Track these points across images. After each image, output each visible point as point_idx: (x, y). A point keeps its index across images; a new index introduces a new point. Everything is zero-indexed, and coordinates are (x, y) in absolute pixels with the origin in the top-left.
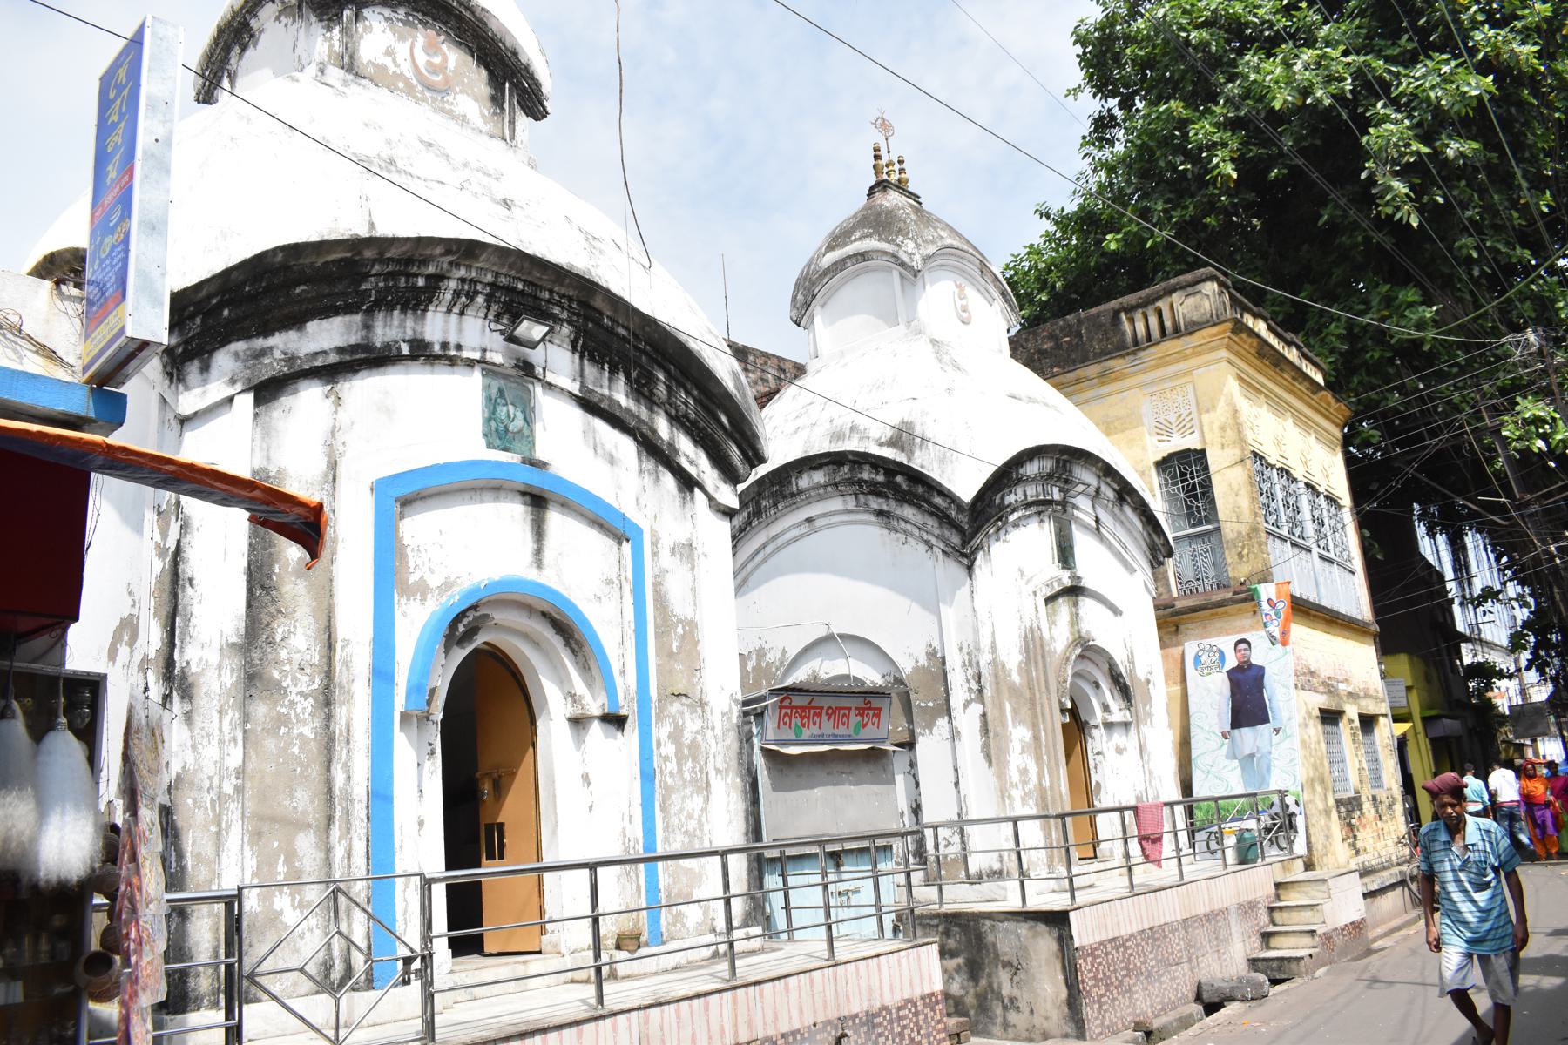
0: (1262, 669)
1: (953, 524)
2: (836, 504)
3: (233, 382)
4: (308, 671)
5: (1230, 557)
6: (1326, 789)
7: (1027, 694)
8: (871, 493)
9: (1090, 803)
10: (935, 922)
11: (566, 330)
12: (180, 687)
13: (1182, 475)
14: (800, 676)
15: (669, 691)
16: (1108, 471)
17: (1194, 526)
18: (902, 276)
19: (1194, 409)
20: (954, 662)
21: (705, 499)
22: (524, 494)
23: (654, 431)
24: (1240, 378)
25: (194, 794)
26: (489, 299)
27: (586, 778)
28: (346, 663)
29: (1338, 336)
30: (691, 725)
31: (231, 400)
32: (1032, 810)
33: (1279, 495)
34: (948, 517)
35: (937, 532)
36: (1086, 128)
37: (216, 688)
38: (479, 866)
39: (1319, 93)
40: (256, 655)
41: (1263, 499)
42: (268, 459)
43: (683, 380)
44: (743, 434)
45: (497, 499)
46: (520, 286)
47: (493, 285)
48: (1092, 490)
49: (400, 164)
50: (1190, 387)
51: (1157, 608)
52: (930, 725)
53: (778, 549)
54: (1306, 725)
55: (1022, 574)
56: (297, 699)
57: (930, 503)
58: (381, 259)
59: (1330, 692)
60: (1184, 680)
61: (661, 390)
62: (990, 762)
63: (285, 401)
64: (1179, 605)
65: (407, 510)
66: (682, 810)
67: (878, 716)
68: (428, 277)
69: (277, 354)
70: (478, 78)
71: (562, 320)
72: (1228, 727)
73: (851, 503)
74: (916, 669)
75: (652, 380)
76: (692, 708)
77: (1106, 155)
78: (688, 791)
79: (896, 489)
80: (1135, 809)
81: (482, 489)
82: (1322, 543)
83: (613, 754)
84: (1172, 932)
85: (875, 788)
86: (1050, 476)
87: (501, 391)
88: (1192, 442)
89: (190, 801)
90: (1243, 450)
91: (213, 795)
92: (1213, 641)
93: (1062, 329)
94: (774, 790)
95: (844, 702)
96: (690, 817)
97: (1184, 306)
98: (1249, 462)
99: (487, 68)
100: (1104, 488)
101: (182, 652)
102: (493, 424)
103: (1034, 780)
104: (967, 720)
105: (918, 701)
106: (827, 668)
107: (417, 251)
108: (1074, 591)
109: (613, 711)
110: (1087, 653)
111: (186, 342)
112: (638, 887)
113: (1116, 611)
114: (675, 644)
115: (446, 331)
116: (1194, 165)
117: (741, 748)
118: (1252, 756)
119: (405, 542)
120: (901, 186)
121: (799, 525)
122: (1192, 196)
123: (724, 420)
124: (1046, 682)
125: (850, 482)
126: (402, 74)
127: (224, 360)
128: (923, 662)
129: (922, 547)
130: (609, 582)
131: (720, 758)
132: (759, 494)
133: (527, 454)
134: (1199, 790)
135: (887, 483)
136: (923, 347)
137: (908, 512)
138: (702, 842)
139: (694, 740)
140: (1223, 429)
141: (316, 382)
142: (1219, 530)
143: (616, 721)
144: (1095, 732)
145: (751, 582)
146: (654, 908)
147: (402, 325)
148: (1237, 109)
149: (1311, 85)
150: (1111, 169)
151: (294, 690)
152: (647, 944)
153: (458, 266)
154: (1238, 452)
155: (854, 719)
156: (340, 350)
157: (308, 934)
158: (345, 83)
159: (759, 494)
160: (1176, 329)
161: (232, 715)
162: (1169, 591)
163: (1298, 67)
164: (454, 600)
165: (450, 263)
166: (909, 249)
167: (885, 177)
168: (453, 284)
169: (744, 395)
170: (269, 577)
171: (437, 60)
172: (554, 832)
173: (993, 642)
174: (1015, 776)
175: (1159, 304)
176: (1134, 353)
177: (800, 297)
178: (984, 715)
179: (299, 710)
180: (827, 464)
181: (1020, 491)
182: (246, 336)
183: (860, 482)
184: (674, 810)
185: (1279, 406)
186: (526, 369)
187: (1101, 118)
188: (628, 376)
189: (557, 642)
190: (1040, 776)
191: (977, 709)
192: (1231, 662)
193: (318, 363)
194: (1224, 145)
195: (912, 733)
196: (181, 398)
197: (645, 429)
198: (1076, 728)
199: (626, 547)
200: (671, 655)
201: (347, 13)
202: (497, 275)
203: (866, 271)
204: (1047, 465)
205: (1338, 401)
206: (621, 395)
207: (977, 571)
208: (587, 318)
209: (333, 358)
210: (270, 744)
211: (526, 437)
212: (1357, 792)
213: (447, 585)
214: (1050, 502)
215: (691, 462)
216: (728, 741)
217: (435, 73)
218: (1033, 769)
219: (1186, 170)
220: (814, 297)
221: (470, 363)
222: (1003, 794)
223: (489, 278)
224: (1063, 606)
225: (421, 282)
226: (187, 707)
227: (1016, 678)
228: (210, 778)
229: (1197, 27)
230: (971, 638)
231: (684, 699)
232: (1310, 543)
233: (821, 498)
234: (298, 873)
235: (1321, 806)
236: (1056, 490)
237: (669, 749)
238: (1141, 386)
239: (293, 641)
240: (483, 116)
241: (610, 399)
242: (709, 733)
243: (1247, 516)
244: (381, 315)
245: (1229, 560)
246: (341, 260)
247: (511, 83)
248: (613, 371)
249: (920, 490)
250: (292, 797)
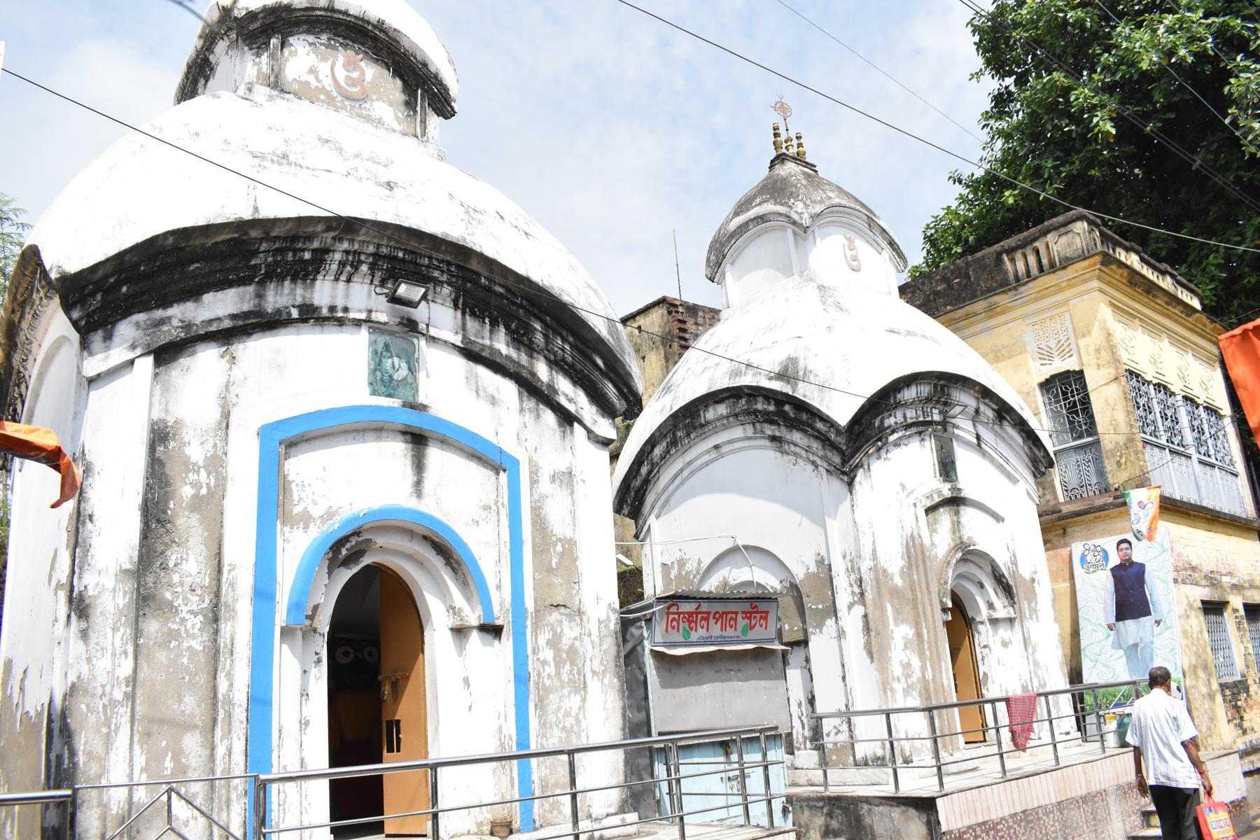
0: (1142, 566)
1: (834, 446)
2: (738, 432)
3: (133, 347)
4: (199, 592)
5: (1109, 465)
6: (1209, 675)
7: (910, 596)
8: (766, 421)
9: (979, 694)
10: (821, 804)
11: (446, 290)
12: (77, 608)
13: (1064, 393)
14: (711, 585)
15: (547, 603)
16: (985, 393)
17: (1074, 439)
18: (795, 233)
19: (1071, 335)
20: (839, 568)
21: (584, 432)
22: (404, 433)
23: (534, 375)
24: (1112, 304)
25: (88, 700)
26: (373, 267)
27: (466, 681)
28: (232, 585)
29: (1218, 266)
30: (569, 632)
31: (132, 362)
32: (915, 702)
33: (1157, 409)
34: (828, 439)
35: (821, 453)
36: (987, 105)
37: (110, 608)
38: (381, 762)
39: (1182, 52)
40: (150, 579)
41: (1141, 412)
42: (167, 411)
43: (558, 328)
44: (618, 374)
45: (379, 439)
46: (401, 255)
47: (376, 255)
48: (971, 411)
49: (292, 158)
50: (1067, 316)
51: (1040, 516)
52: (820, 625)
53: (692, 473)
54: (1188, 617)
55: (904, 488)
56: (188, 616)
57: (813, 428)
58: (267, 238)
59: (1212, 585)
60: (1072, 577)
61: (539, 339)
62: (872, 658)
63: (184, 361)
64: (1066, 509)
65: (293, 451)
66: (559, 708)
67: (766, 618)
68: (314, 251)
69: (175, 322)
70: (394, 88)
71: (442, 282)
72: (1113, 620)
73: (750, 430)
74: (808, 575)
75: (529, 330)
76: (571, 618)
77: (1001, 125)
78: (565, 691)
79: (784, 415)
80: (1007, 700)
81: (364, 430)
82: (1203, 450)
83: (493, 658)
84: (1047, 814)
86: (928, 400)
87: (387, 346)
88: (1071, 364)
89: (83, 706)
90: (1117, 369)
91: (105, 700)
92: (1097, 542)
93: (953, 272)
95: (732, 607)
96: (567, 714)
97: (1057, 244)
98: (1123, 379)
99: (402, 78)
100: (983, 408)
101: (80, 578)
102: (379, 374)
103: (917, 673)
104: (851, 620)
105: (809, 604)
106: (737, 575)
107: (300, 229)
108: (955, 502)
109: (487, 622)
110: (969, 557)
111: (88, 316)
112: (512, 779)
113: (998, 518)
114: (554, 561)
115: (333, 297)
116: (1077, 126)
117: (618, 652)
118: (1136, 645)
119: (290, 478)
120: (799, 159)
121: (708, 452)
122: (1078, 152)
123: (599, 362)
124: (927, 584)
125: (748, 412)
126: (323, 87)
127: (126, 330)
128: (813, 569)
129: (810, 467)
130: (487, 508)
131: (596, 662)
132: (675, 426)
133: (410, 399)
134: (1089, 677)
135: (777, 411)
136: (811, 292)
137: (797, 436)
138: (579, 737)
139: (572, 646)
140: (1098, 351)
141: (213, 344)
142: (1098, 442)
143: (492, 630)
144: (981, 627)
145: (673, 499)
146: (527, 799)
147: (292, 293)
148: (1114, 74)
149: (1175, 46)
150: (1007, 136)
151: (185, 609)
152: (519, 831)
153: (341, 240)
154: (1112, 371)
155: (742, 623)
156: (233, 317)
157: (192, 822)
158: (271, 98)
159: (675, 426)
160: (1052, 265)
161: (126, 631)
162: (1056, 497)
163: (1162, 30)
164: (334, 528)
165: (334, 238)
166: (801, 210)
167: (784, 150)
168: (338, 256)
169: (618, 340)
170: (165, 512)
171: (355, 75)
172: (437, 730)
173: (874, 550)
174: (897, 670)
175: (1036, 244)
176: (1015, 288)
177: (713, 257)
178: (866, 616)
179: (189, 626)
180: (728, 398)
181: (899, 414)
182: (147, 308)
183: (756, 412)
184: (551, 708)
185: (1154, 329)
186: (411, 326)
187: (1000, 94)
188: (507, 328)
189: (437, 562)
190: (923, 669)
191: (859, 610)
192: (1115, 560)
193: (213, 328)
194: (1103, 106)
195: (805, 631)
196: (85, 363)
197: (524, 373)
198: (960, 622)
199: (503, 477)
200: (550, 570)
201: (274, 41)
202: (379, 246)
203: (766, 231)
204: (925, 390)
205: (1213, 321)
206: (501, 345)
208: (465, 280)
209: (227, 324)
210: (162, 656)
211: (411, 383)
212: (1243, 676)
213: (329, 515)
214: (930, 423)
215: (570, 400)
216: (605, 646)
217: (353, 85)
218: (916, 663)
219: (1071, 131)
220: (724, 257)
221: (358, 323)
222: (885, 687)
223: (371, 249)
224: (945, 516)
225: (307, 256)
226: (84, 625)
227: (898, 581)
228: (103, 686)
229: (1073, 8)
230: (853, 547)
231: (562, 610)
232: (1192, 451)
233: (725, 428)
234: (184, 769)
235: (1204, 690)
236: (936, 411)
237: (548, 654)
238: (1024, 317)
239: (184, 566)
240: (397, 118)
241: (491, 348)
242: (586, 639)
243: (1124, 428)
244: (273, 285)
245: (1108, 468)
246: (229, 240)
247: (423, 89)
248: (494, 324)
249: (804, 417)
250: (180, 701)
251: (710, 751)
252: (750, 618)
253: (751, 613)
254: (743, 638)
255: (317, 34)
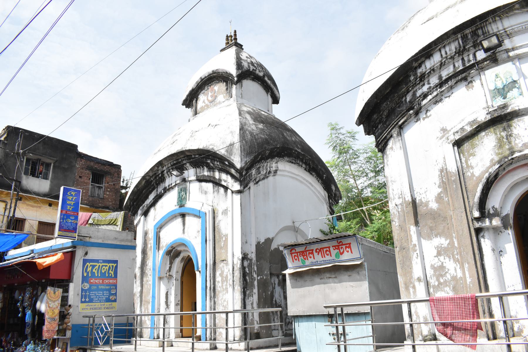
66: (222, 298)
67: (350, 247)
85: (351, 284)
94: (292, 288)
95: (326, 245)
96: (225, 301)
155: (334, 252)
206: (206, 173)
207: (388, 150)
223: (170, 165)
241: (203, 175)
251: (323, 319)
252: (338, 249)
253: (338, 246)
254: (337, 259)
255: (204, 89)
